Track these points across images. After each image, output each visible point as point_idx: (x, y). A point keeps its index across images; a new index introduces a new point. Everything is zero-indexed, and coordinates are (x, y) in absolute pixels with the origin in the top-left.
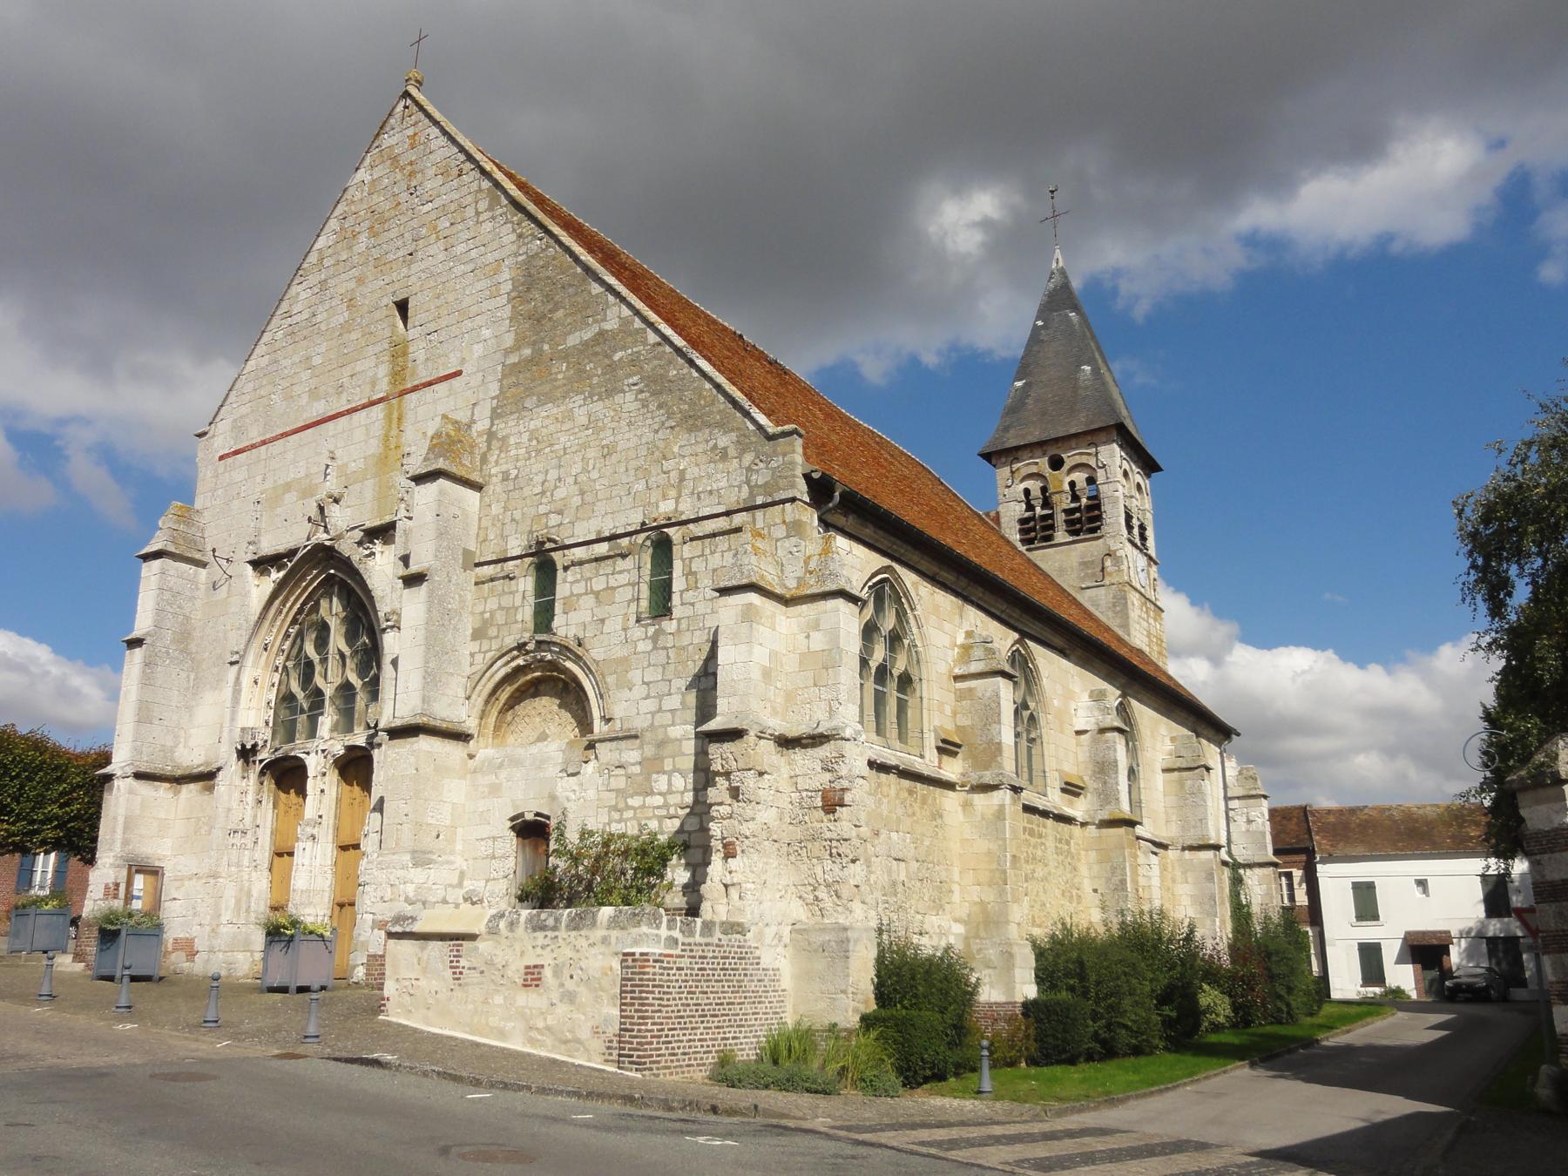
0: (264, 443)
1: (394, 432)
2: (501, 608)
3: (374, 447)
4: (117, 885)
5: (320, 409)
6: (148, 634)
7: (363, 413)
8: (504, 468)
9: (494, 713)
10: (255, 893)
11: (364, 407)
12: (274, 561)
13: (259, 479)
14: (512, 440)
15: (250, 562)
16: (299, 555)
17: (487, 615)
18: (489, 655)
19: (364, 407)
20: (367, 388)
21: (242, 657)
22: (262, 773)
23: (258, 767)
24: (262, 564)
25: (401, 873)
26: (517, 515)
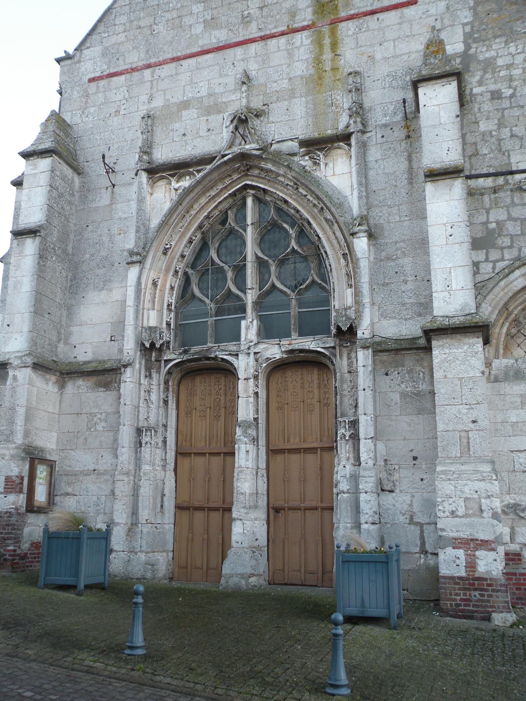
0: (149, 66)
1: (327, 56)
2: (510, 218)
3: (301, 67)
4: (22, 478)
5: (221, 36)
6: (41, 226)
7: (283, 40)
8: (492, 87)
9: (507, 324)
10: (166, 492)
11: (282, 34)
12: (177, 168)
13: (144, 98)
14: (500, 62)
15: (144, 170)
16: (216, 163)
17: (493, 225)
18: (500, 265)
19: (282, 34)
20: (286, 19)
21: (145, 257)
22: (169, 373)
23: (164, 370)
24: (155, 172)
25: (481, 486)
26: (519, 130)
